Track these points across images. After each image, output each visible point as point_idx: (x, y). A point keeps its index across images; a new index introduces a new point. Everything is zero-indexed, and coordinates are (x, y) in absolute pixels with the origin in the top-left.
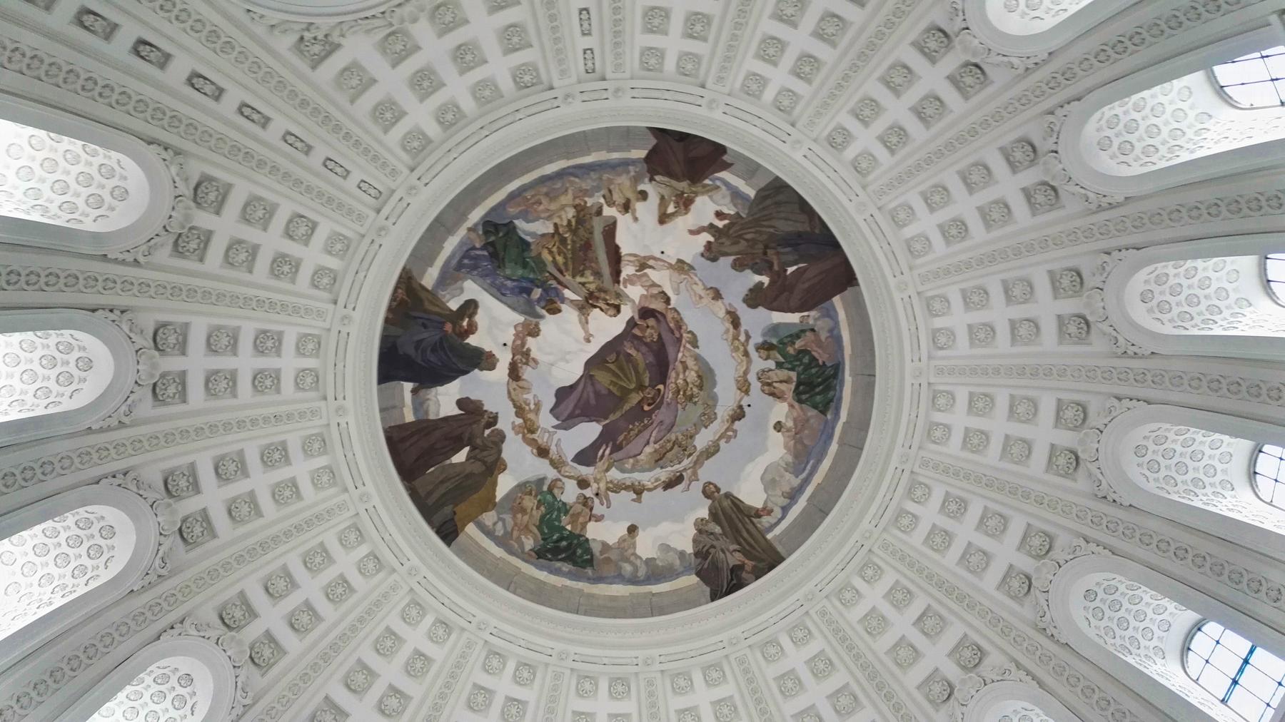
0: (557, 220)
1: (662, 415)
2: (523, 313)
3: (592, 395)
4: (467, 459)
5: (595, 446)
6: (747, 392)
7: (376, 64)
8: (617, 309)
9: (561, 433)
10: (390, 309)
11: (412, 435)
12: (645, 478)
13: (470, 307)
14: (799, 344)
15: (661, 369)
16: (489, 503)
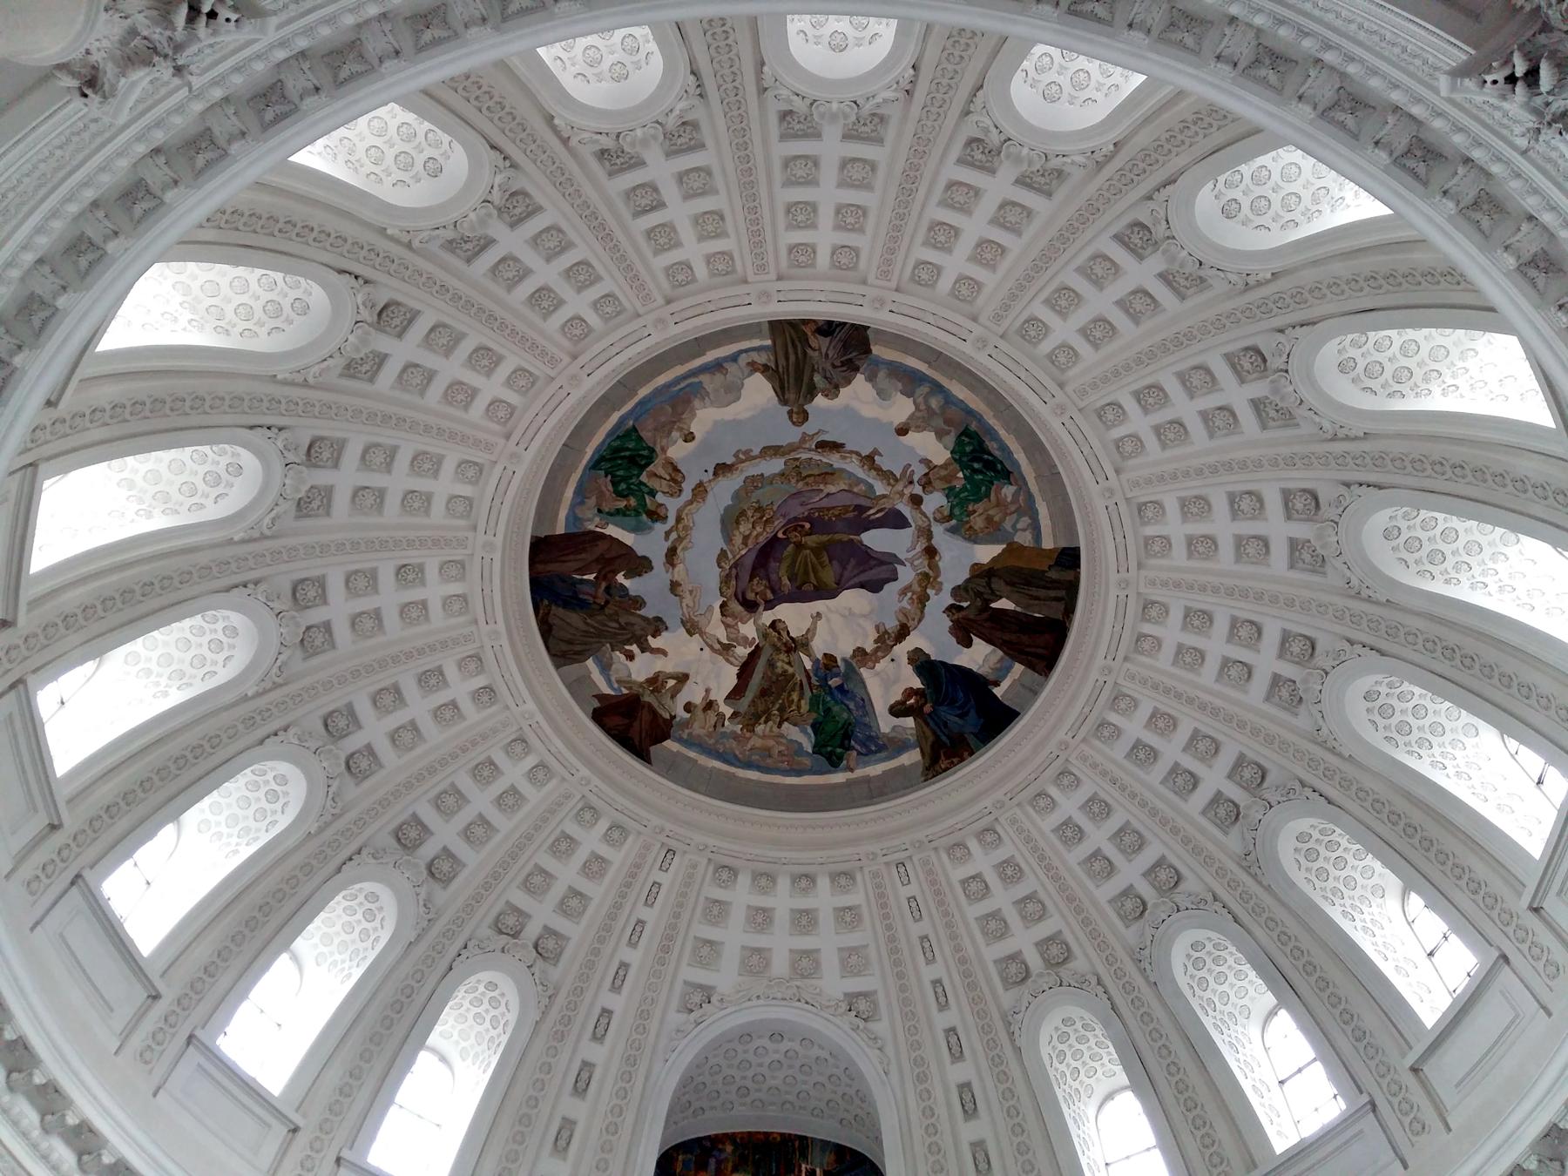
0: (775, 729)
1: (797, 511)
2: (859, 675)
3: (849, 567)
6: (700, 484)
7: (830, 962)
8: (773, 625)
9: (902, 556)
10: (962, 760)
11: (1028, 654)
12: (854, 467)
13: (897, 710)
14: (622, 504)
15: (767, 553)
16: (1013, 549)
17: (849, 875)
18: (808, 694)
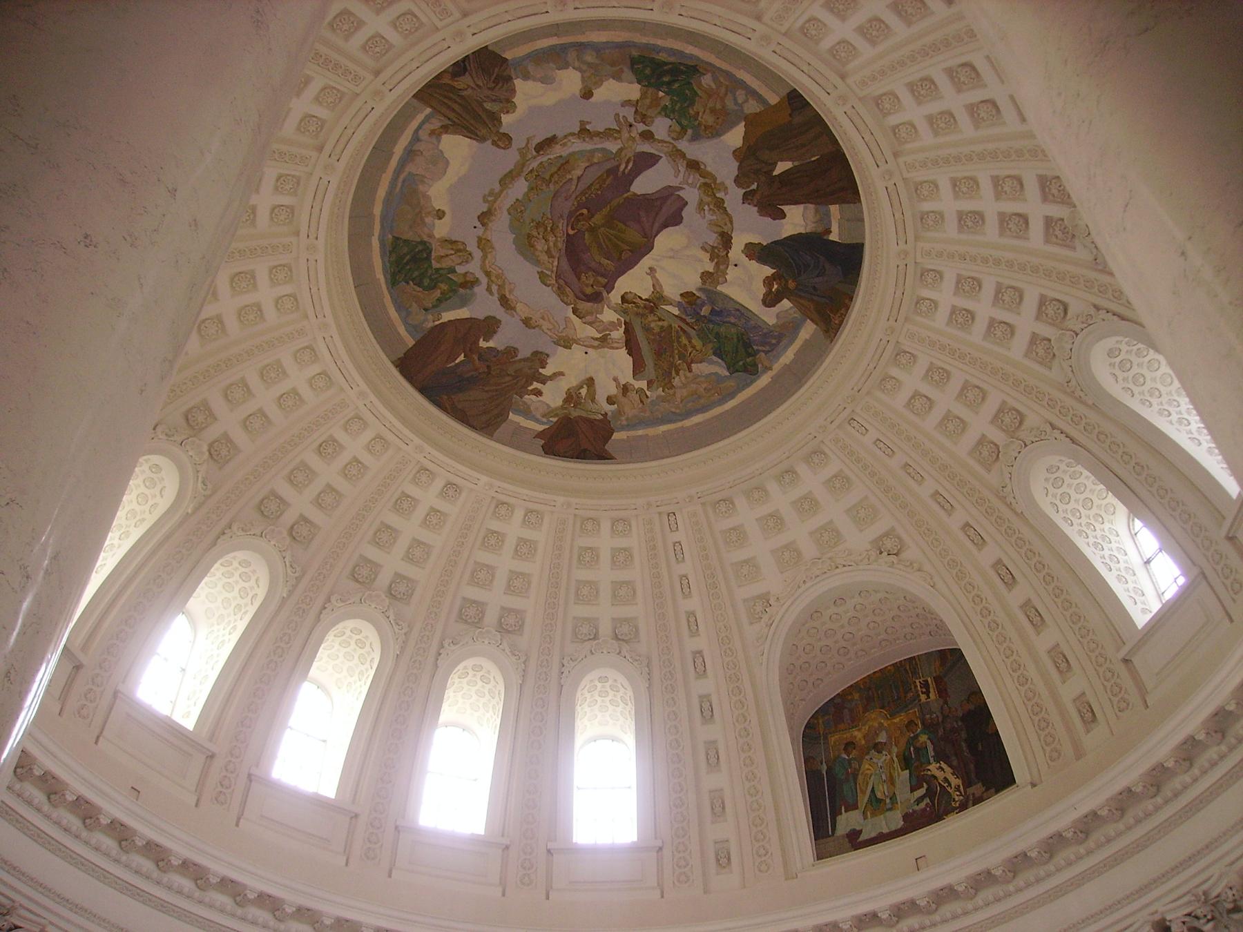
0: (688, 374)
4: (776, 164)
5: (636, 172)
6: (480, 239)
9: (675, 182)
12: (577, 145)
13: (770, 300)
14: (437, 294)
15: (573, 250)
16: (752, 122)
17: (818, 452)
18: (693, 333)
